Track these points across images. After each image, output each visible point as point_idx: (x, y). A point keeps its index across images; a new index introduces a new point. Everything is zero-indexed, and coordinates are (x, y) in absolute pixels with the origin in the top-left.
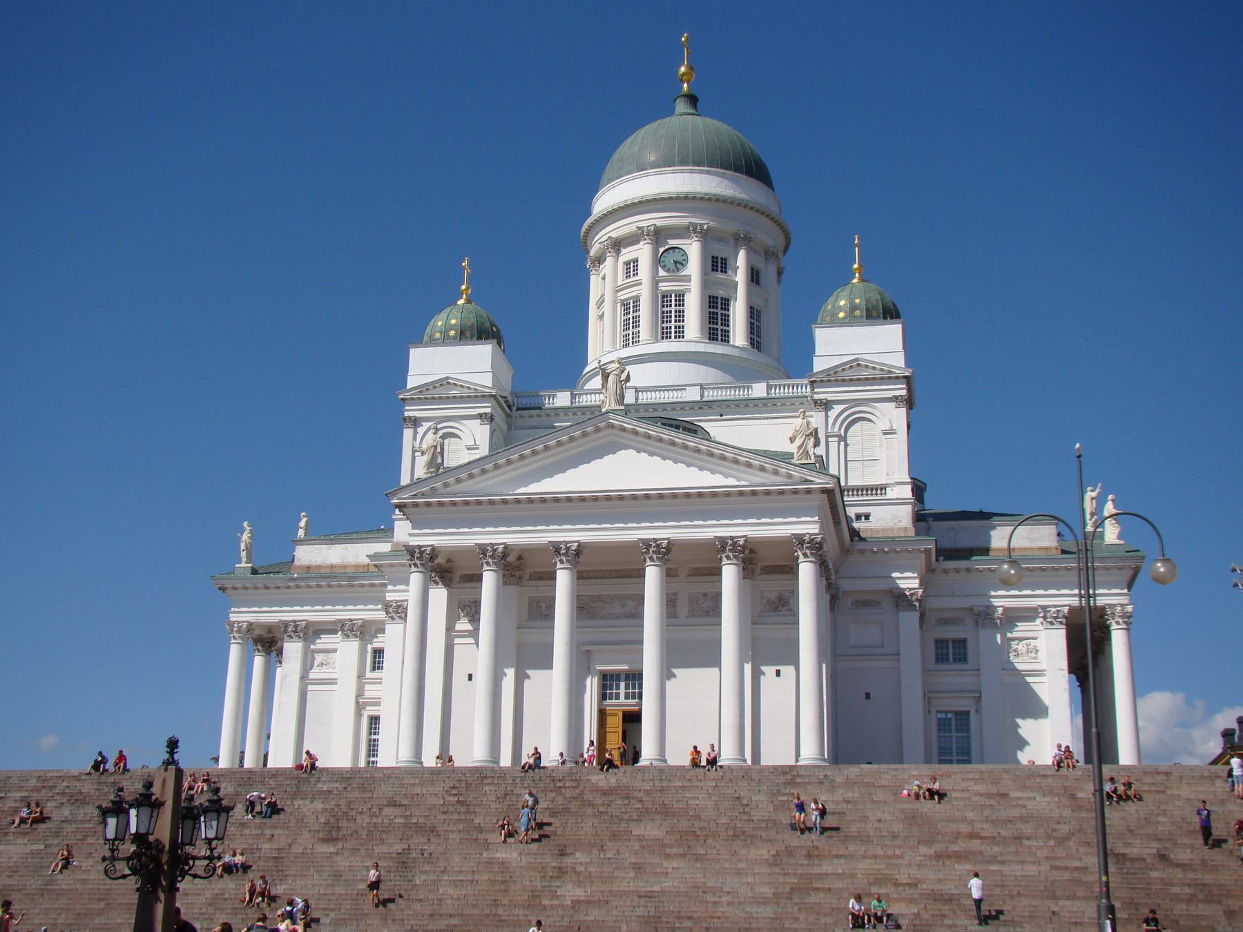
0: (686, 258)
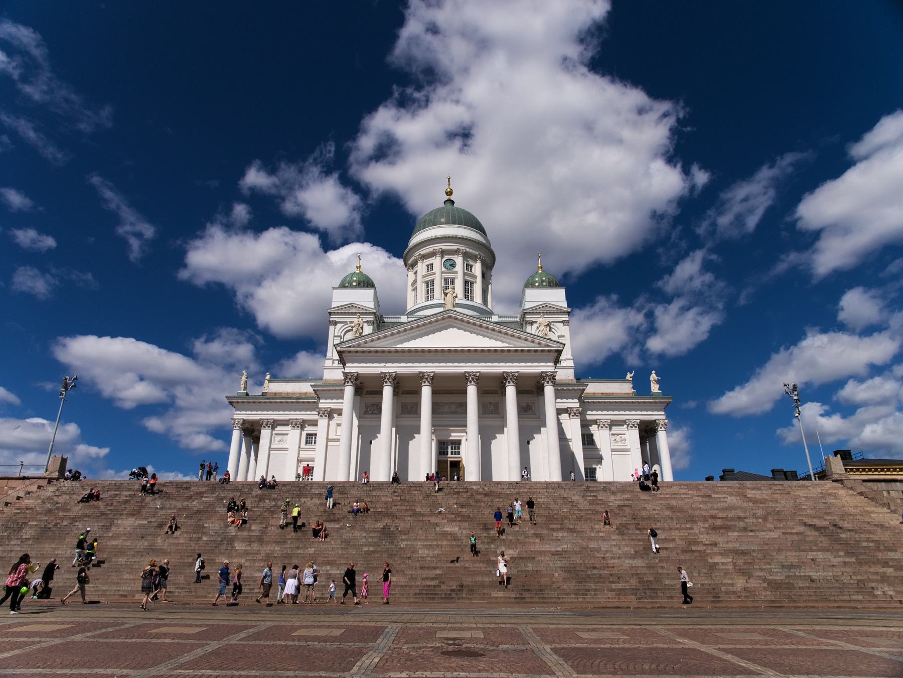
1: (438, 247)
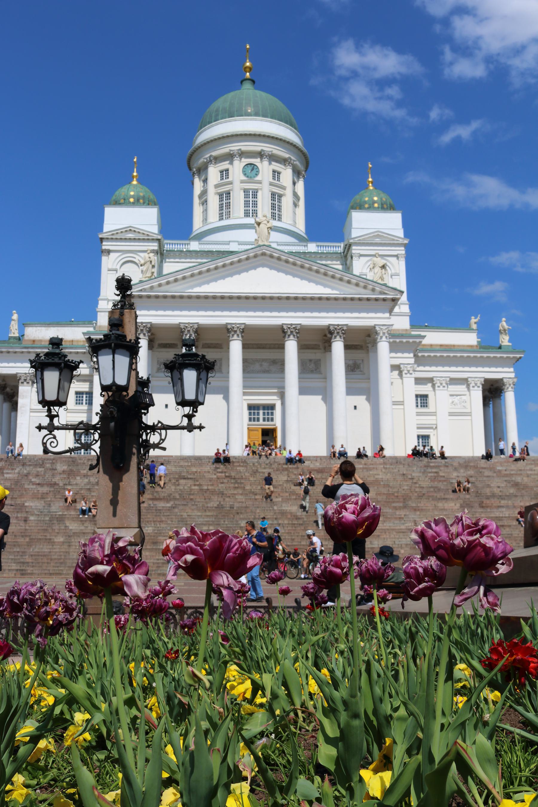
0: (257, 170)
1: (235, 147)
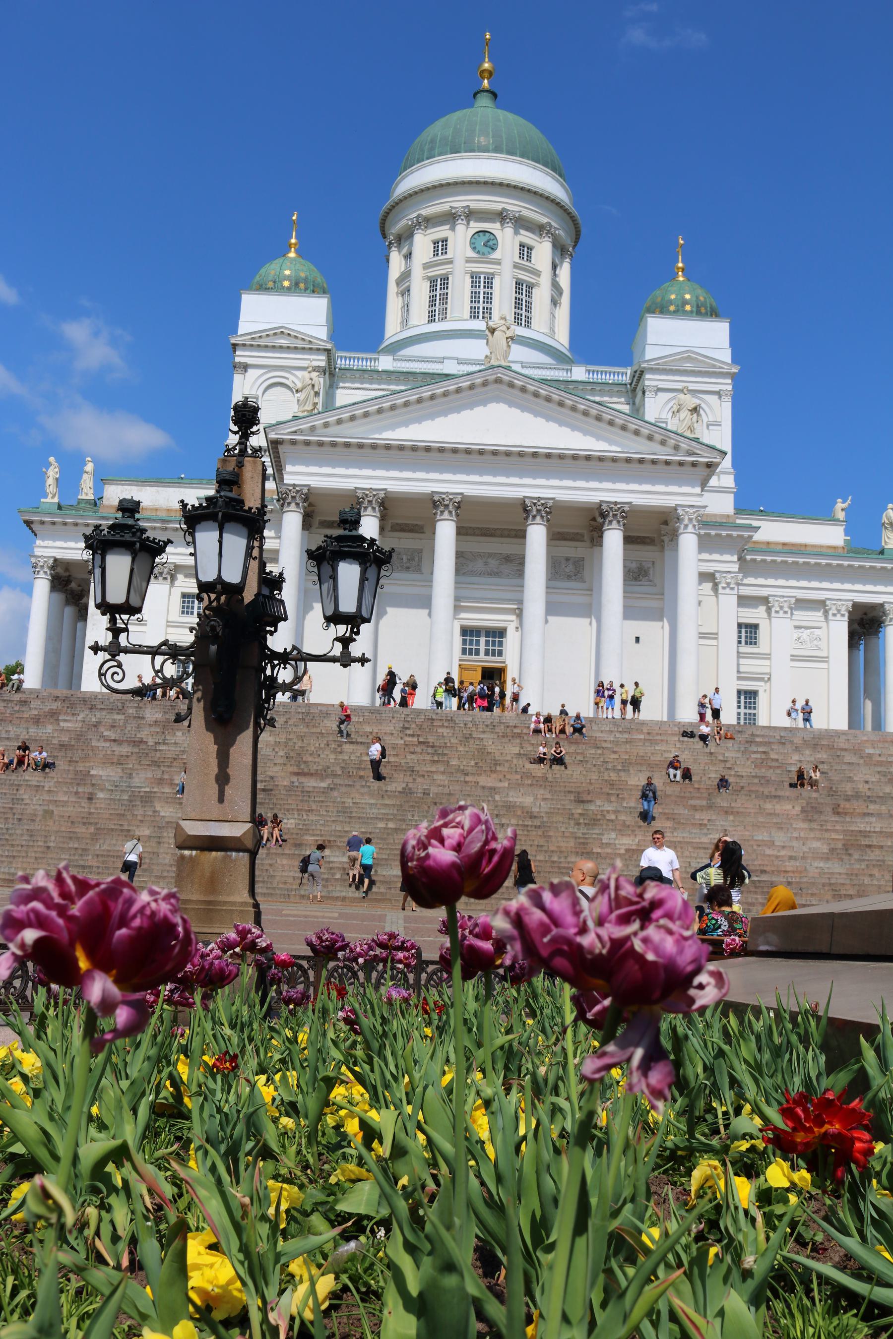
0: (495, 242)
